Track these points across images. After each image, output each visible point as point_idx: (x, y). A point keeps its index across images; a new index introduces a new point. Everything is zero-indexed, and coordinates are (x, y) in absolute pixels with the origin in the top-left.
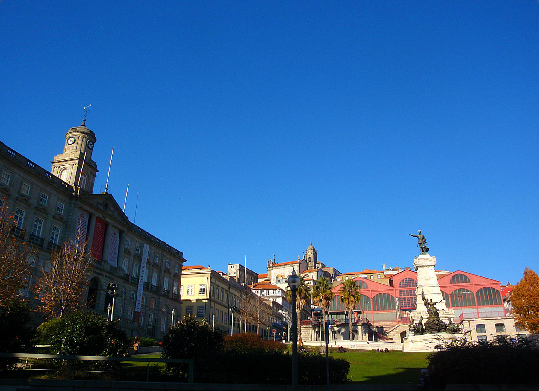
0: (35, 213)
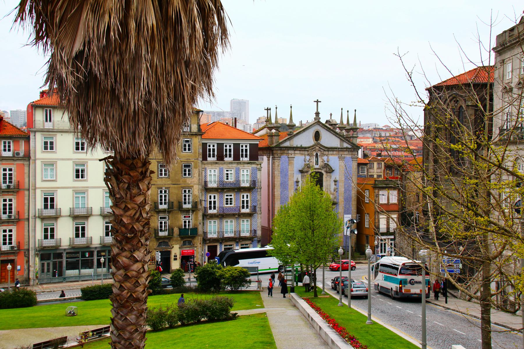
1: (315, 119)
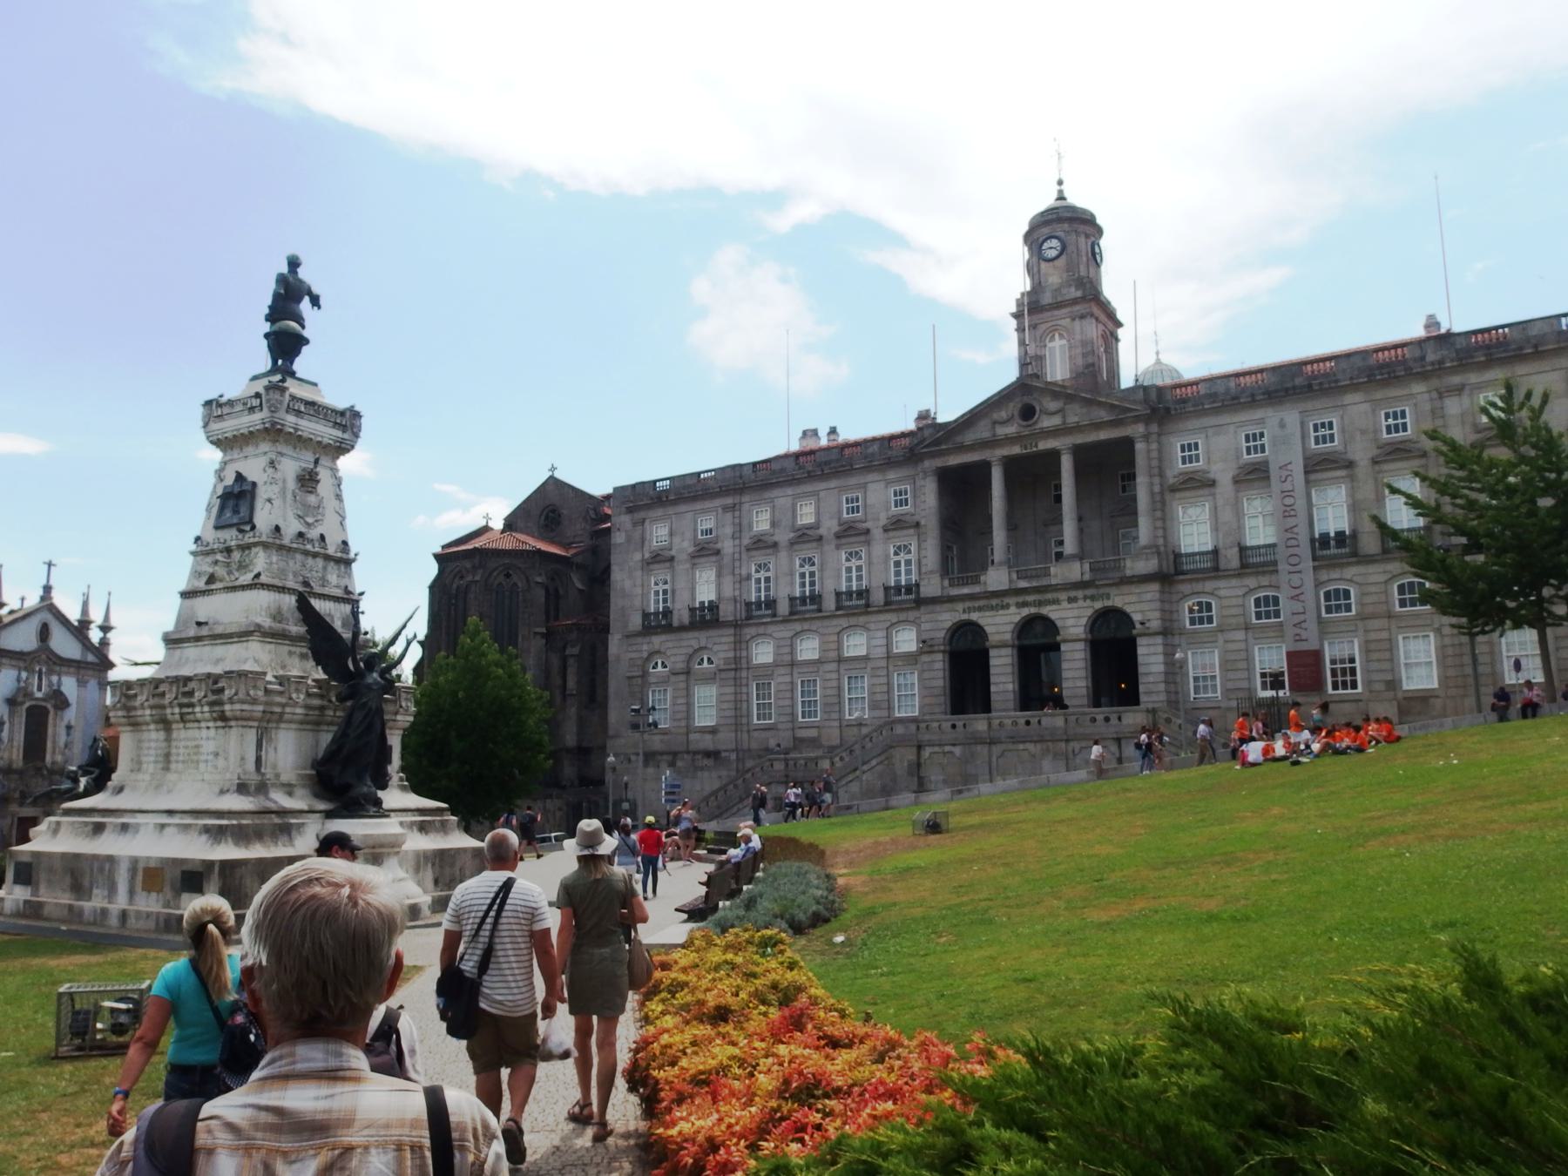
0: (838, 547)
1: (43, 599)
